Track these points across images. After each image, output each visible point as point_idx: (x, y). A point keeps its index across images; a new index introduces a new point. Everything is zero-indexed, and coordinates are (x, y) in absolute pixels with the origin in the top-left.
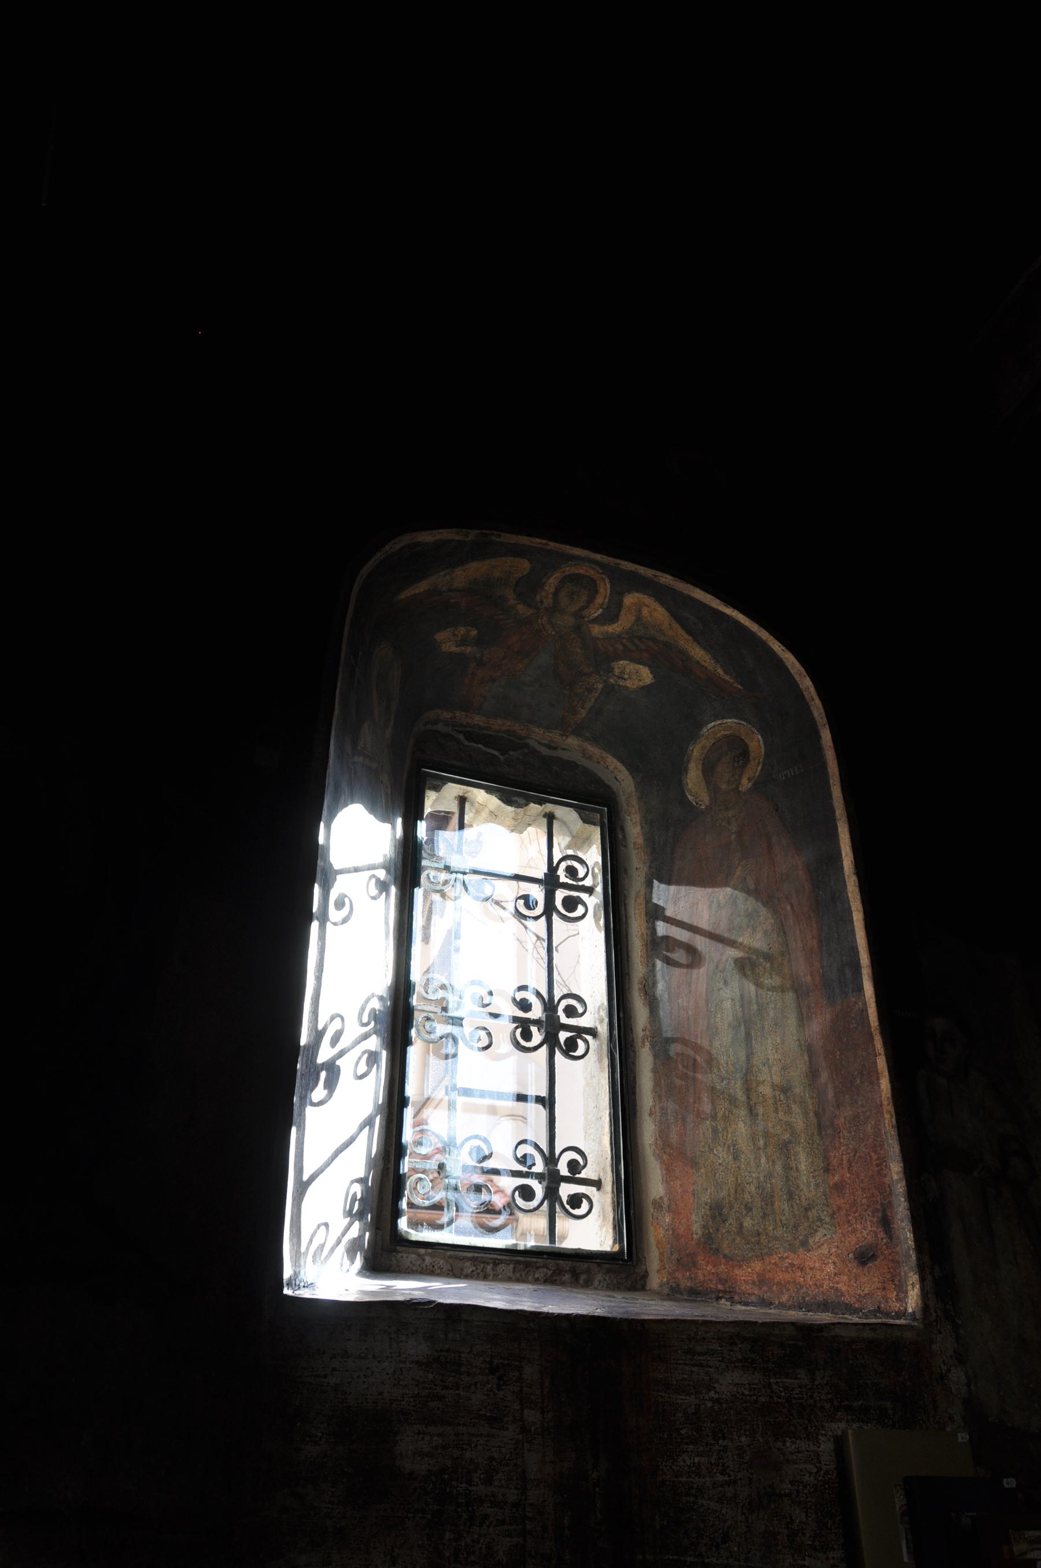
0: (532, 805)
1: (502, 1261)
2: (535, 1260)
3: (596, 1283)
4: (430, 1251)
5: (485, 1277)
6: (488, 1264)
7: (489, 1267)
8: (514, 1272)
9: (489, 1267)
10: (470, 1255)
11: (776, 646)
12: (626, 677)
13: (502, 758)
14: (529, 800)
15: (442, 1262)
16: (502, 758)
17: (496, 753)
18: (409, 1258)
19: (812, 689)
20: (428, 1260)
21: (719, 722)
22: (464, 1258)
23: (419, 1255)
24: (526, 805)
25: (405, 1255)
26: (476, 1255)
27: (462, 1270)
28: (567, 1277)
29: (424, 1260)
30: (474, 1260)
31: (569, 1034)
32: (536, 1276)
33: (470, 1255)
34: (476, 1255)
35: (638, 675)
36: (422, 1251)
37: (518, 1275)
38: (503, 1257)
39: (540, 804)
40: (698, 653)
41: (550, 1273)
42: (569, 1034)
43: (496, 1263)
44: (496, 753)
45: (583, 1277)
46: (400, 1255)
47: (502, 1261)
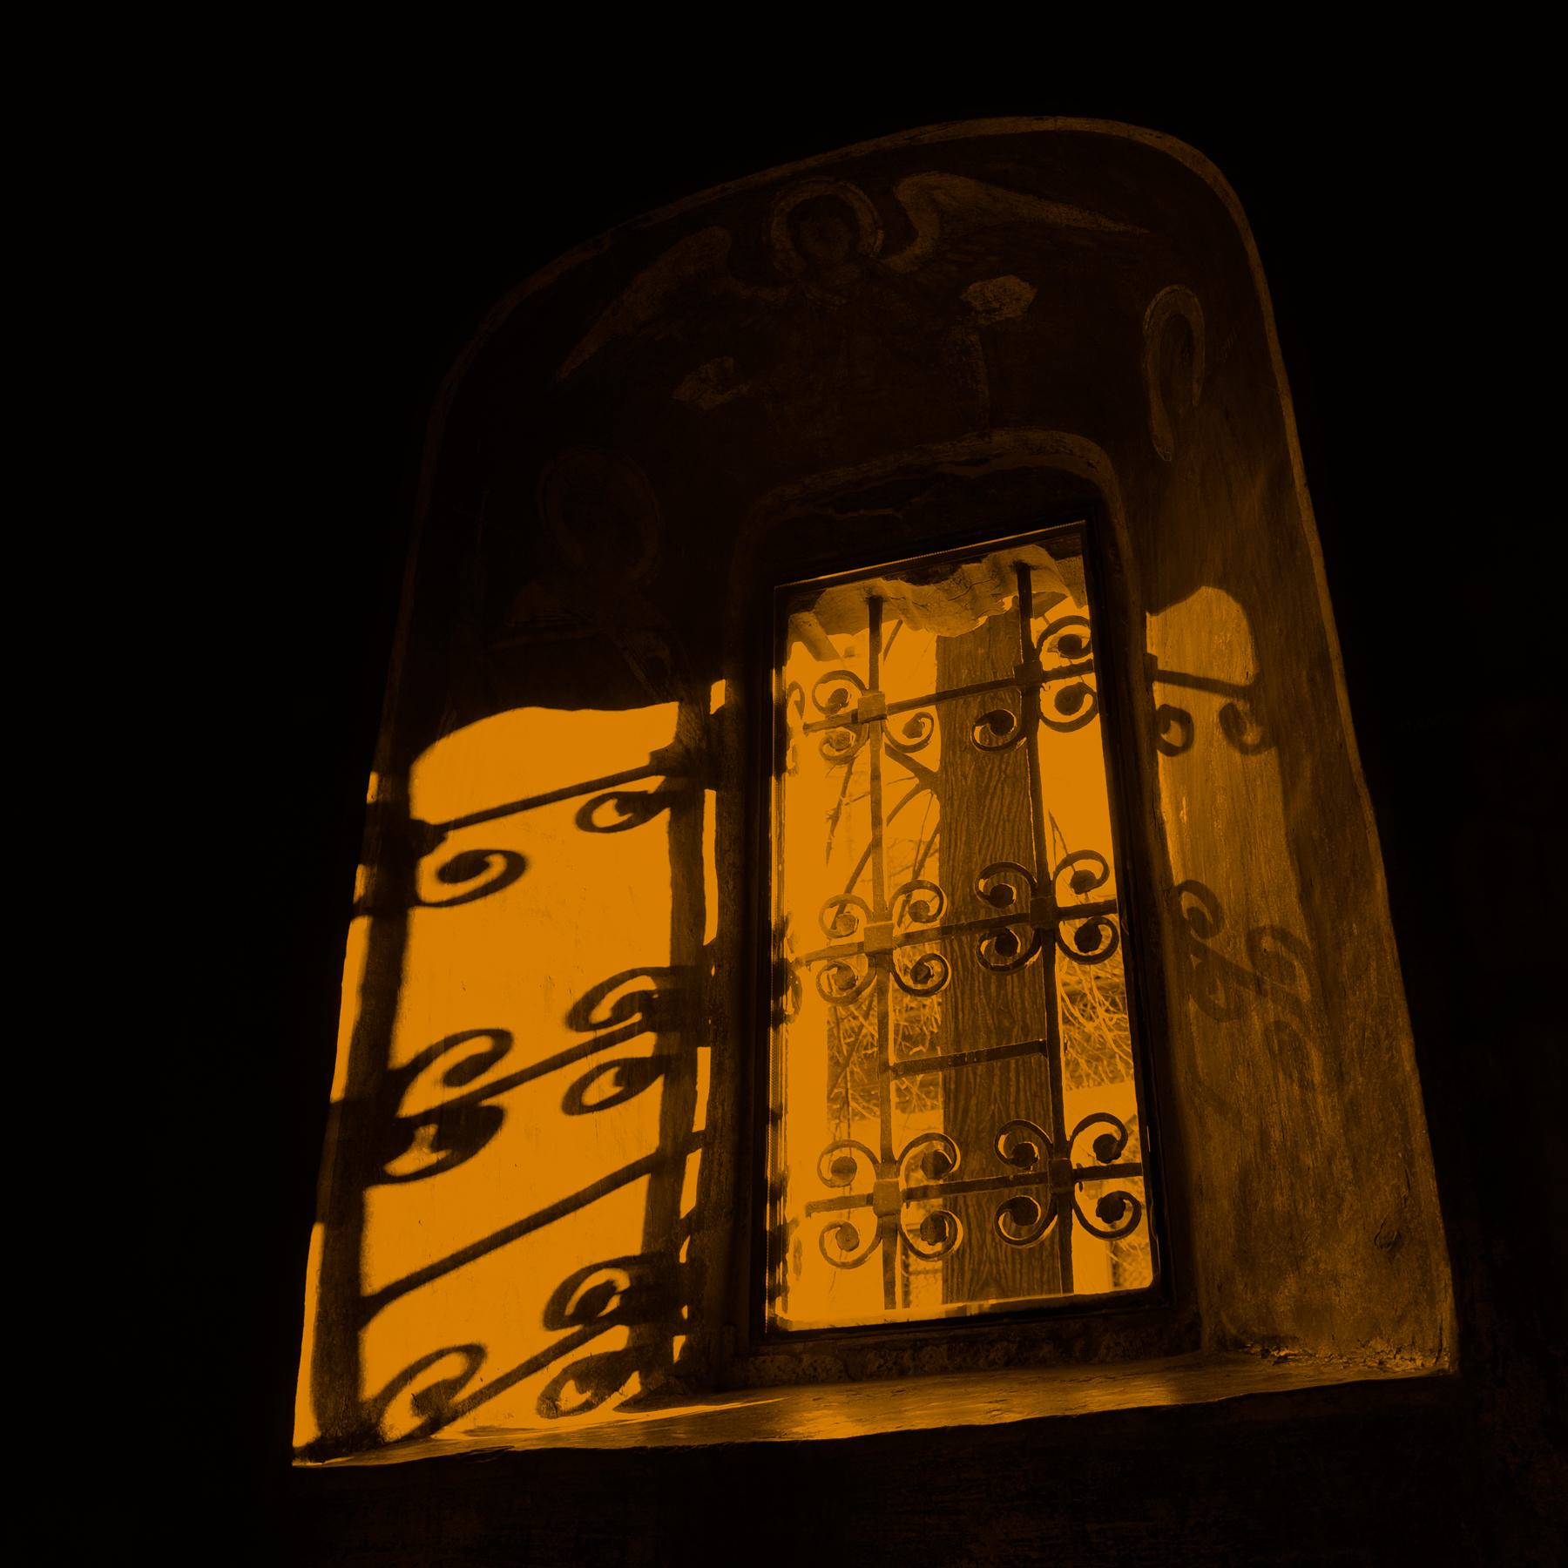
0: (965, 567)
2: (987, 1329)
5: (903, 1374)
7: (907, 1355)
9: (907, 1355)
10: (871, 1341)
11: (1147, 137)
12: (997, 305)
14: (956, 562)
19: (1222, 179)
20: (807, 1359)
21: (1153, 303)
24: (953, 572)
26: (885, 1338)
29: (800, 1361)
31: (1079, 923)
32: (992, 1356)
33: (871, 1341)
34: (885, 1338)
35: (1009, 295)
36: (799, 1347)
38: (935, 1335)
39: (978, 560)
40: (1060, 214)
42: (1079, 923)
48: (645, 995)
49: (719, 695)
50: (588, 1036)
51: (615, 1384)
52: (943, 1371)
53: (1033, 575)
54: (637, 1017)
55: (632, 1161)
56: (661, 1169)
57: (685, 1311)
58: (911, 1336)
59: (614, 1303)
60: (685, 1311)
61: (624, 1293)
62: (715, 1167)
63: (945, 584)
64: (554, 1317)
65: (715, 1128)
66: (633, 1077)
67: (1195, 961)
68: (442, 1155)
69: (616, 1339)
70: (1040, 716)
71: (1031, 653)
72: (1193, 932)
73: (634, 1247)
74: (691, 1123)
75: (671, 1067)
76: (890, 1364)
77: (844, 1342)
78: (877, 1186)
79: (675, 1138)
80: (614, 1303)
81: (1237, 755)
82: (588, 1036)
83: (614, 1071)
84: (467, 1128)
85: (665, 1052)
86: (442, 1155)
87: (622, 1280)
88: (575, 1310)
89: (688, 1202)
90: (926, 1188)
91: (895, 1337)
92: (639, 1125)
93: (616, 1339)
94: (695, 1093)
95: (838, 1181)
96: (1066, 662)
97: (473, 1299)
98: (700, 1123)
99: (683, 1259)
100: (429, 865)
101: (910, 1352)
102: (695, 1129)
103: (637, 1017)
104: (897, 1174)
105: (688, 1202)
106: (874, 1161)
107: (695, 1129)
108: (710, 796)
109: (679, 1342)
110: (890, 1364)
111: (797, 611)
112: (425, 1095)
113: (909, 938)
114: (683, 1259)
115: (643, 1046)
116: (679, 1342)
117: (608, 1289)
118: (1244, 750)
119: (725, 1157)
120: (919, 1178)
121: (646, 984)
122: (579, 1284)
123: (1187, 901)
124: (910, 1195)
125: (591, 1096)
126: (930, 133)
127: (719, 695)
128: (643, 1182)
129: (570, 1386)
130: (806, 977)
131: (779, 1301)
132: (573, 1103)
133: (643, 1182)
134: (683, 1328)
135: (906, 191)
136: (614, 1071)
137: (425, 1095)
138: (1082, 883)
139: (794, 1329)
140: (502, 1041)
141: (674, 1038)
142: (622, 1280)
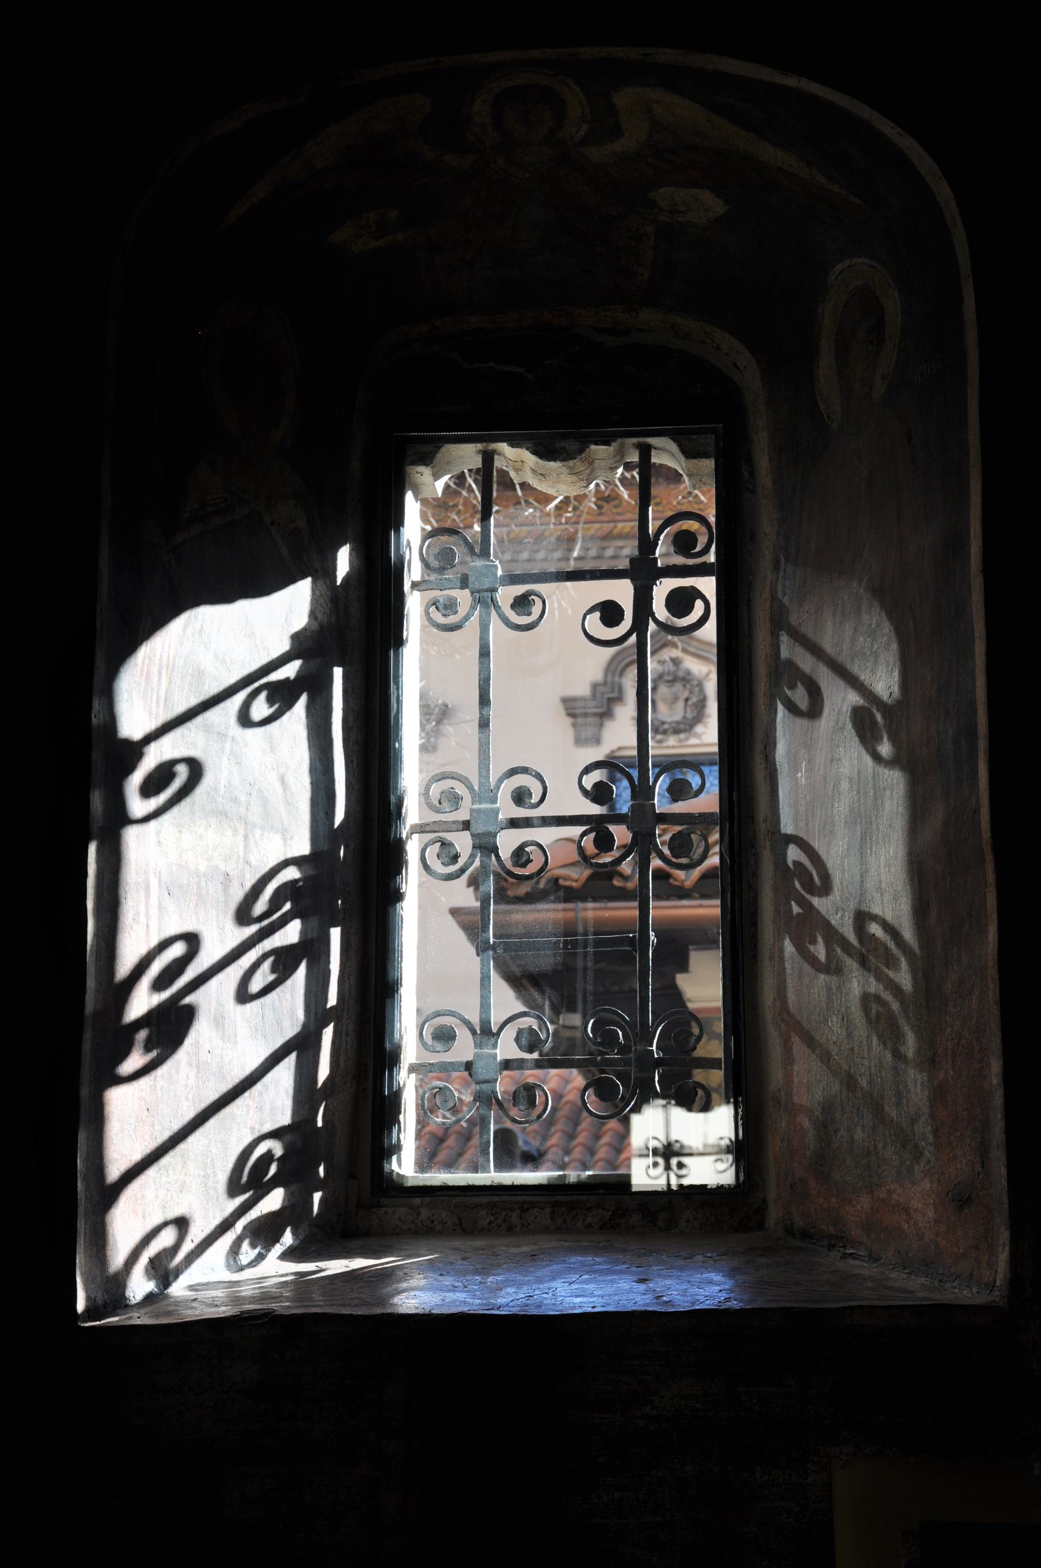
15: (444, 1214)
38: (539, 1198)
39: (607, 443)
48: (294, 882)
50: (254, 929)
51: (276, 1239)
53: (653, 452)
55: (287, 1038)
56: (303, 1046)
57: (321, 1170)
59: (273, 1169)
60: (321, 1170)
61: (280, 1159)
62: (344, 1038)
64: (234, 1187)
65: (344, 1001)
66: (284, 962)
67: (796, 909)
68: (154, 1054)
69: (274, 1201)
70: (653, 615)
71: (647, 544)
72: (797, 885)
73: (285, 1118)
74: (326, 999)
75: (312, 949)
77: (458, 1200)
78: (476, 1055)
79: (316, 1014)
80: (273, 1169)
81: (868, 760)
82: (254, 929)
83: (271, 959)
84: (171, 1026)
85: (309, 937)
86: (154, 1054)
87: (277, 1148)
88: (248, 1179)
89: (324, 1071)
90: (522, 1060)
92: (288, 1007)
94: (329, 971)
95: (439, 1046)
96: (679, 560)
97: (181, 1185)
98: (332, 1000)
99: (320, 1124)
100: (137, 778)
102: (329, 1006)
104: (495, 1046)
105: (324, 1071)
106: (473, 1032)
107: (329, 1006)
112: (142, 1001)
113: (514, 823)
114: (320, 1124)
117: (268, 1157)
118: (877, 757)
119: (351, 1027)
120: (515, 1053)
122: (248, 1159)
123: (793, 853)
124: (507, 1065)
125: (256, 984)
126: (666, 56)
128: (293, 1056)
129: (245, 1245)
130: (413, 849)
131: (394, 1158)
133: (293, 1056)
134: (319, 1185)
135: (623, 98)
136: (271, 959)
137: (142, 1001)
138: (679, 791)
139: (410, 1184)
140: (192, 940)
141: (314, 922)
142: (277, 1148)
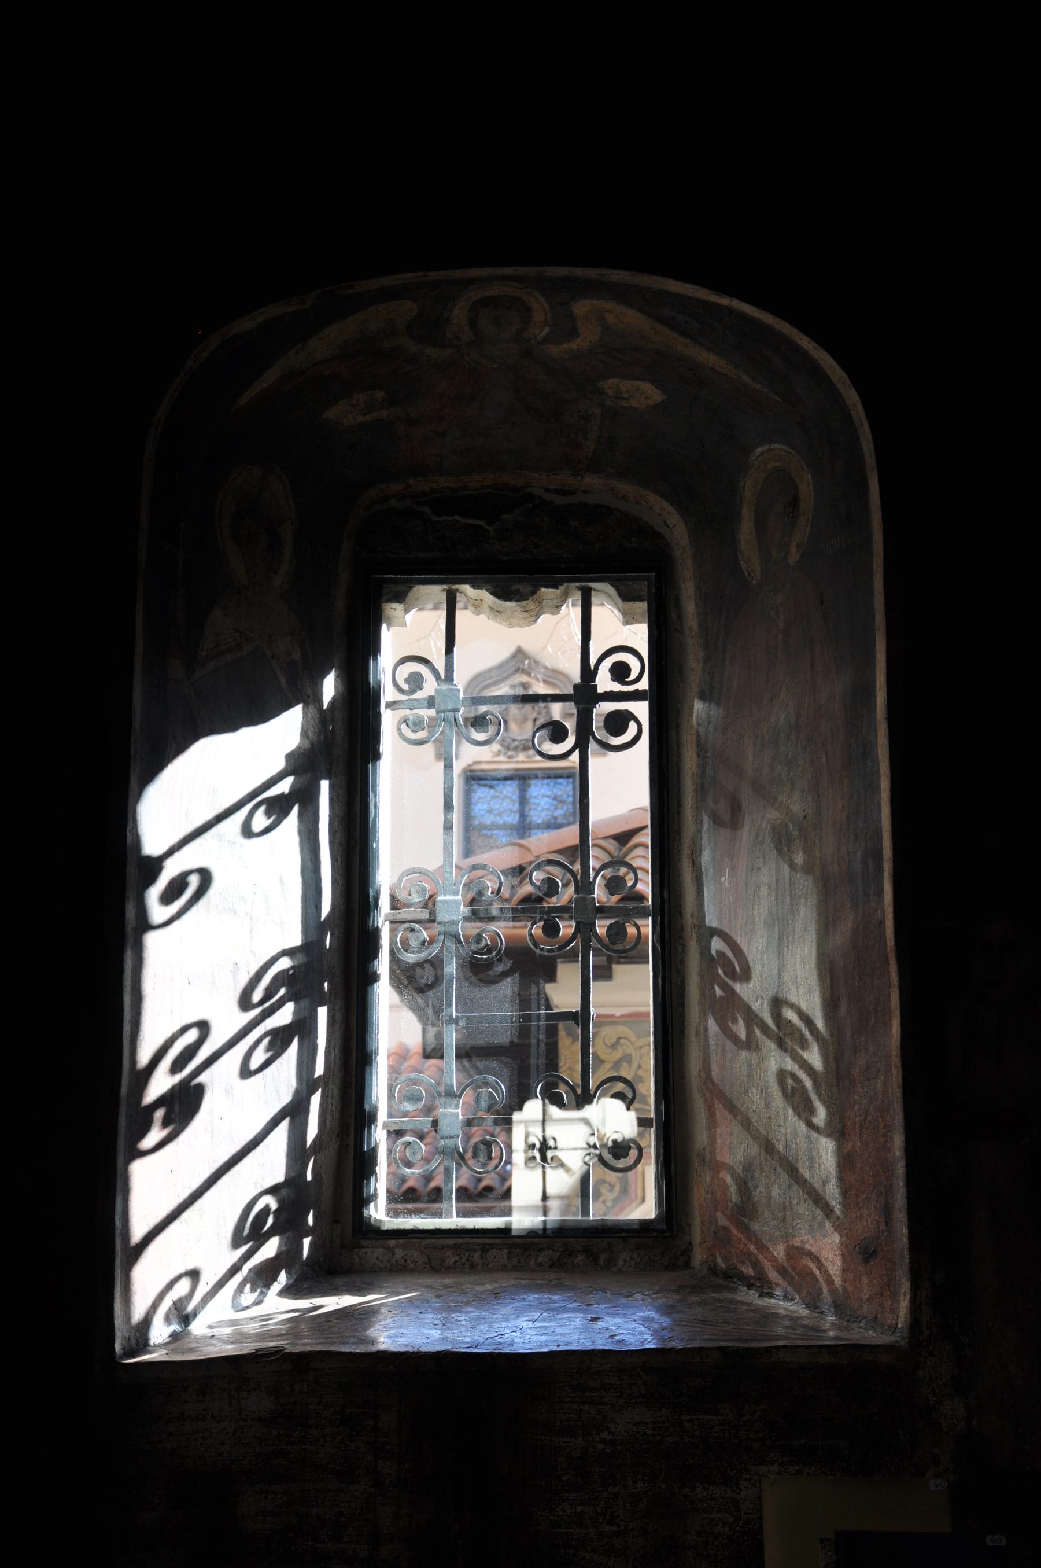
1: (492, 1246)
3: (621, 1263)
4: (402, 1241)
6: (475, 1251)
7: (477, 1255)
8: (509, 1258)
9: (477, 1255)
10: (451, 1242)
13: (491, 529)
16: (491, 529)
17: (482, 523)
18: (374, 1253)
20: (399, 1253)
22: (443, 1247)
23: (388, 1248)
24: (533, 593)
25: (369, 1251)
27: (443, 1261)
28: (580, 1258)
29: (394, 1254)
30: (456, 1247)
32: (540, 1260)
34: (460, 1241)
36: (392, 1243)
37: (515, 1261)
41: (556, 1255)
43: (485, 1249)
44: (482, 523)
45: (603, 1257)
46: (364, 1250)
47: (492, 1246)
49: (329, 687)
52: (504, 1268)
54: (282, 991)
58: (480, 1241)
59: (270, 1221)
63: (524, 603)
66: (279, 1040)
76: (463, 1261)
80: (270, 1221)
88: (250, 1232)
91: (467, 1240)
92: (282, 1079)
93: (271, 1248)
99: (309, 1178)
101: (479, 1252)
103: (282, 991)
108: (325, 785)
109: (307, 1242)
110: (463, 1261)
111: (389, 601)
114: (309, 1178)
115: (285, 1016)
116: (307, 1242)
121: (285, 963)
127: (329, 687)
131: (372, 1205)
132: (246, 1072)
